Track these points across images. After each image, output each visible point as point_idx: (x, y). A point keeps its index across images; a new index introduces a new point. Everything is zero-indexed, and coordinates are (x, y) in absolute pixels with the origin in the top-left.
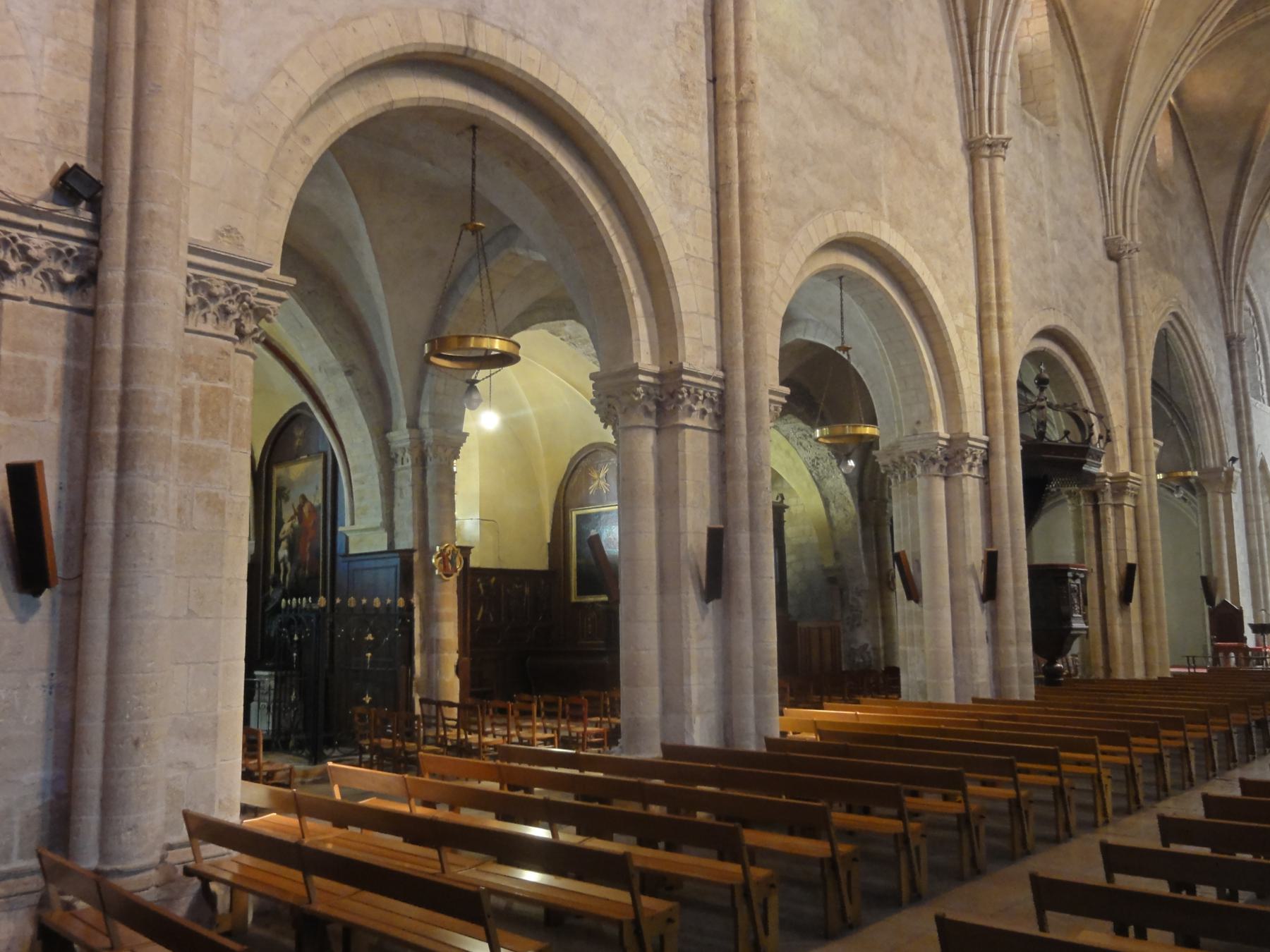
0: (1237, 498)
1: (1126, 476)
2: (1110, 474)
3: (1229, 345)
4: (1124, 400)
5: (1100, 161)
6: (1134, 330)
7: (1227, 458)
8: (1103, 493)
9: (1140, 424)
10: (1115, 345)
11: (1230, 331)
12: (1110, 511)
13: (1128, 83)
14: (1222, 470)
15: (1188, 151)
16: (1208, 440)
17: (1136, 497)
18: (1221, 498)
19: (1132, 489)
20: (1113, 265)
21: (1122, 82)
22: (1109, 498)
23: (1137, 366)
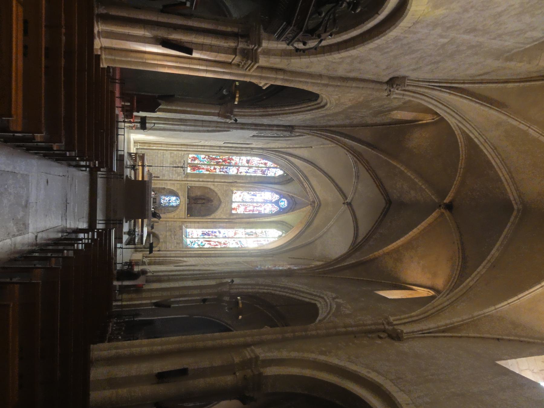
0: (215, 118)
1: (256, 60)
2: (259, 50)
3: (289, 126)
4: (304, 70)
5: (451, 83)
6: (344, 84)
7: (237, 118)
8: (247, 42)
9: (286, 78)
10: (341, 72)
11: (296, 127)
12: (232, 44)
13: (491, 108)
14: (232, 115)
15: (390, 124)
16: (247, 111)
17: (238, 65)
18: (217, 111)
19: (245, 64)
20: (386, 79)
21: (491, 104)
22: (241, 45)
23: (323, 82)
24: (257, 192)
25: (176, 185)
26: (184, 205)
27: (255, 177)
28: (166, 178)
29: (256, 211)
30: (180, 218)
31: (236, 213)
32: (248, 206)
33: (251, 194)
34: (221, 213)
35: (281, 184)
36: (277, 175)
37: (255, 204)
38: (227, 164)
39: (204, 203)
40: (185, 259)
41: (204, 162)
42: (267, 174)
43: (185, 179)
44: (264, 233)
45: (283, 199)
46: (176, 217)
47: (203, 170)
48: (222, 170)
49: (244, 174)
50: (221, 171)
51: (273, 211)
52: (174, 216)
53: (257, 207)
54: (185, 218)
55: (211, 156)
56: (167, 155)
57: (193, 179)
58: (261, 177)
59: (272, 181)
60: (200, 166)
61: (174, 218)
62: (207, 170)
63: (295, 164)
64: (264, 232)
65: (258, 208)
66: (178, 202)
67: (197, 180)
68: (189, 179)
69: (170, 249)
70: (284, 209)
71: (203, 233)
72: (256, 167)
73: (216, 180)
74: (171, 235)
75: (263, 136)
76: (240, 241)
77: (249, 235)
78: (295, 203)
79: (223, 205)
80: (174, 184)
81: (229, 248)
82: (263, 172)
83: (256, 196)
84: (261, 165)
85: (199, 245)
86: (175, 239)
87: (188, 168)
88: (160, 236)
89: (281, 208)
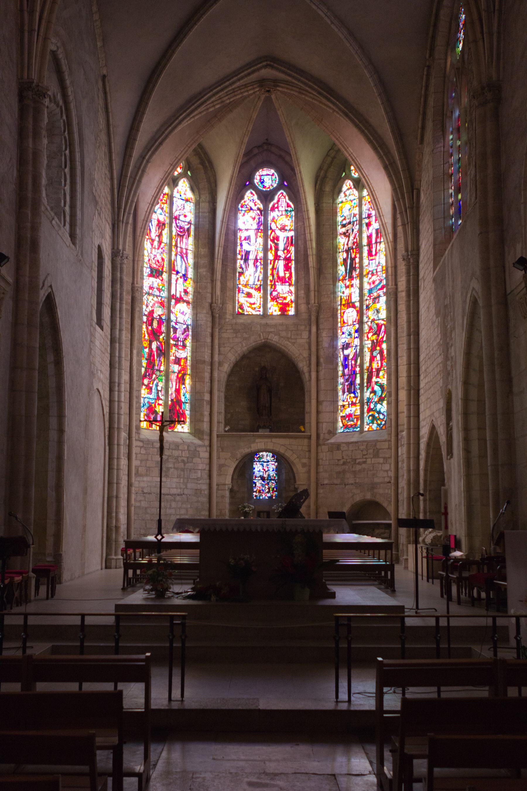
3: (21, 97)
24: (239, 248)
25: (222, 461)
26: (274, 440)
27: (196, 256)
28: (205, 487)
29: (289, 251)
30: (310, 451)
31: (293, 305)
32: (275, 272)
33: (244, 266)
34: (293, 344)
35: (216, 186)
36: (190, 195)
37: (271, 256)
38: (163, 329)
39: (270, 391)
40: (424, 431)
41: (159, 388)
42: (190, 223)
43: (207, 437)
44: (350, 226)
45: (256, 181)
46: (304, 461)
47: (182, 392)
48: (180, 343)
49: (190, 286)
50: (184, 346)
51: (288, 206)
52: (304, 465)
53: (277, 249)
54: (309, 437)
55: (143, 370)
56: (142, 484)
57: (206, 419)
58: (197, 238)
59: (205, 206)
60: (172, 400)
61: (310, 466)
62: (181, 380)
63: (157, 132)
64: (344, 230)
65: (281, 246)
66: (267, 456)
67: (209, 407)
68: (206, 426)
69: (392, 474)
70: (283, 177)
71: (350, 392)
72: (170, 250)
73: (207, 358)
74: (354, 473)
75: (73, 207)
76: (370, 291)
77: (353, 268)
78: (265, 147)
79: (274, 339)
80: (220, 466)
81: (388, 318)
82: (183, 233)
83: (247, 253)
84: (165, 239)
85: (381, 399)
86: (365, 462)
87: (176, 430)
88: (358, 498)
89: (281, 186)
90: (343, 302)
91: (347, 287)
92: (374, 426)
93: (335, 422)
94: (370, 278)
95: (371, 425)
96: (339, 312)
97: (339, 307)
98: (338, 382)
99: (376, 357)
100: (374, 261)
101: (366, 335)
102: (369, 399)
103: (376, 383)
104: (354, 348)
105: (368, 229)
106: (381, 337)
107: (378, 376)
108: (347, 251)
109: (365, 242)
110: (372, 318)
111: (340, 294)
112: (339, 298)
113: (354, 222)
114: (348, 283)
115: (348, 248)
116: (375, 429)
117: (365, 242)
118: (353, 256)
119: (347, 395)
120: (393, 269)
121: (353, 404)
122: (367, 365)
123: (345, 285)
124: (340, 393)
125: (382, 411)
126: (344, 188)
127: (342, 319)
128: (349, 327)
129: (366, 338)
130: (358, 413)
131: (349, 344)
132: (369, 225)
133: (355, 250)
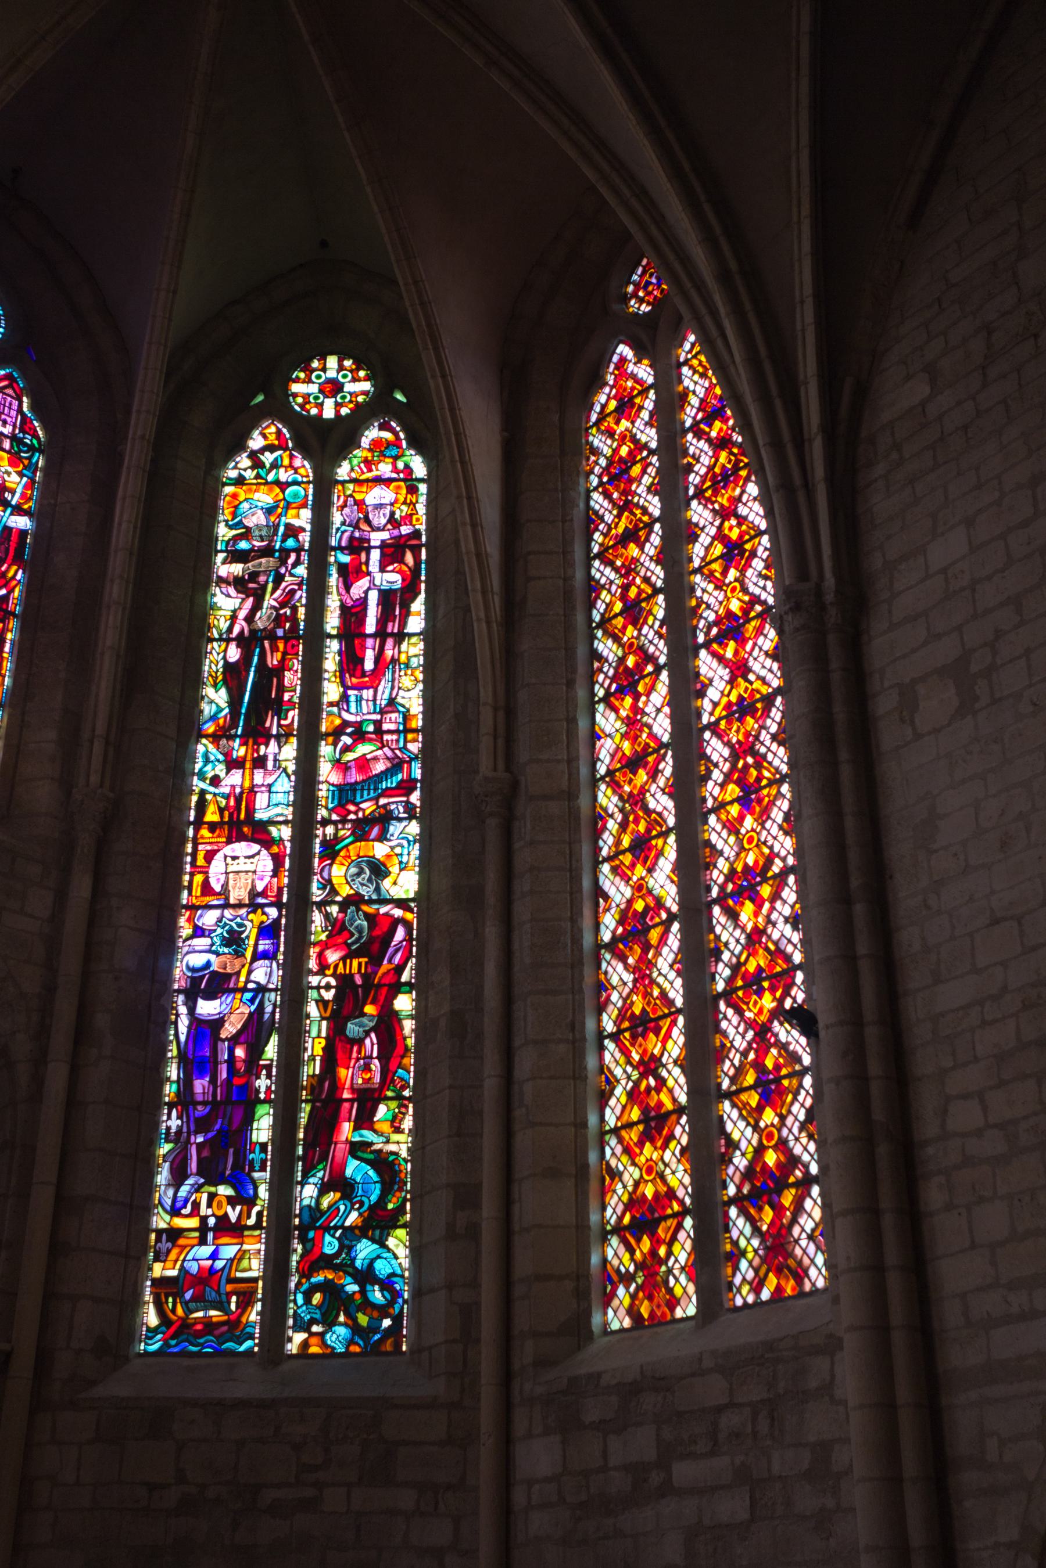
51: (26, 425)
64: (237, 569)
71: (212, 1175)
76: (345, 793)
90: (211, 816)
91: (232, 764)
92: (338, 1336)
93: (136, 1303)
94: (347, 749)
95: (315, 1329)
96: (189, 848)
97: (191, 832)
98: (157, 1124)
99: (360, 1042)
100: (368, 694)
101: (313, 952)
102: (314, 1211)
103: (356, 1149)
104: (248, 995)
105: (348, 587)
106: (385, 966)
107: (365, 1121)
108: (247, 642)
109: (332, 622)
110: (345, 891)
111: (198, 784)
112: (194, 798)
113: (285, 553)
114: (240, 751)
115: (253, 632)
116: (340, 1349)
117: (332, 622)
118: (274, 660)
119: (198, 1189)
120: (501, 714)
121: (226, 1228)
122: (312, 1069)
123: (228, 755)
124: (163, 1177)
125: (382, 1268)
126: (256, 442)
127: (199, 878)
128: (228, 913)
129: (313, 964)
130: (254, 1268)
131: (229, 976)
132: (350, 574)
133: (281, 646)
